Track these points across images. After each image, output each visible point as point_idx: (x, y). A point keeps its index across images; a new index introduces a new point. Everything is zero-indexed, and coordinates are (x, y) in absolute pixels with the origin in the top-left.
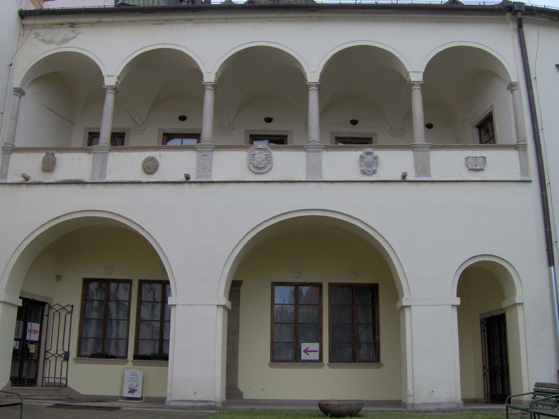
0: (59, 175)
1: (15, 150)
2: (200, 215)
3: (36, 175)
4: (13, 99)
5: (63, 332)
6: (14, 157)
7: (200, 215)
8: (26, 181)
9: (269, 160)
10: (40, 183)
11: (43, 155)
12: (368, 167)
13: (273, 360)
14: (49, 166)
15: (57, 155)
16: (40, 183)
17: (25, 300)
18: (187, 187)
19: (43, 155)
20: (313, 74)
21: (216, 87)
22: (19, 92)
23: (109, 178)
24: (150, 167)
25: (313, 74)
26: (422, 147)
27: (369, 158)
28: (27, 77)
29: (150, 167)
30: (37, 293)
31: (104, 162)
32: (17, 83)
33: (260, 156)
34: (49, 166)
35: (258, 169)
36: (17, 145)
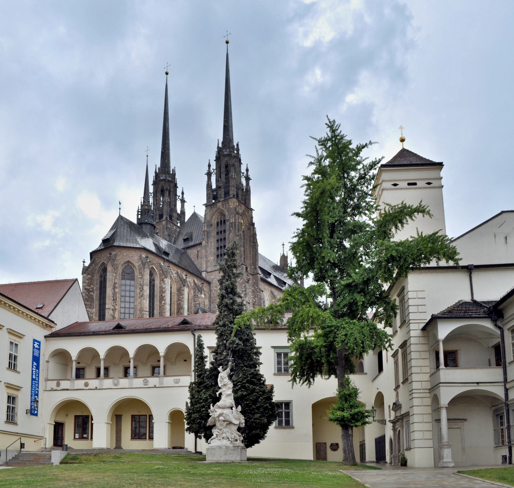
0: (62, 387)
1: (48, 380)
2: (100, 398)
3: (55, 388)
6: (48, 382)
7: (100, 398)
8: (52, 390)
9: (118, 382)
11: (56, 382)
12: (146, 383)
13: (132, 438)
14: (58, 385)
15: (60, 382)
17: (56, 423)
19: (56, 382)
20: (132, 354)
21: (104, 359)
22: (48, 362)
23: (76, 388)
24: (86, 385)
25: (132, 354)
26: (162, 376)
27: (145, 381)
28: (49, 357)
29: (86, 385)
31: (74, 384)
33: (116, 381)
34: (58, 385)
35: (115, 385)
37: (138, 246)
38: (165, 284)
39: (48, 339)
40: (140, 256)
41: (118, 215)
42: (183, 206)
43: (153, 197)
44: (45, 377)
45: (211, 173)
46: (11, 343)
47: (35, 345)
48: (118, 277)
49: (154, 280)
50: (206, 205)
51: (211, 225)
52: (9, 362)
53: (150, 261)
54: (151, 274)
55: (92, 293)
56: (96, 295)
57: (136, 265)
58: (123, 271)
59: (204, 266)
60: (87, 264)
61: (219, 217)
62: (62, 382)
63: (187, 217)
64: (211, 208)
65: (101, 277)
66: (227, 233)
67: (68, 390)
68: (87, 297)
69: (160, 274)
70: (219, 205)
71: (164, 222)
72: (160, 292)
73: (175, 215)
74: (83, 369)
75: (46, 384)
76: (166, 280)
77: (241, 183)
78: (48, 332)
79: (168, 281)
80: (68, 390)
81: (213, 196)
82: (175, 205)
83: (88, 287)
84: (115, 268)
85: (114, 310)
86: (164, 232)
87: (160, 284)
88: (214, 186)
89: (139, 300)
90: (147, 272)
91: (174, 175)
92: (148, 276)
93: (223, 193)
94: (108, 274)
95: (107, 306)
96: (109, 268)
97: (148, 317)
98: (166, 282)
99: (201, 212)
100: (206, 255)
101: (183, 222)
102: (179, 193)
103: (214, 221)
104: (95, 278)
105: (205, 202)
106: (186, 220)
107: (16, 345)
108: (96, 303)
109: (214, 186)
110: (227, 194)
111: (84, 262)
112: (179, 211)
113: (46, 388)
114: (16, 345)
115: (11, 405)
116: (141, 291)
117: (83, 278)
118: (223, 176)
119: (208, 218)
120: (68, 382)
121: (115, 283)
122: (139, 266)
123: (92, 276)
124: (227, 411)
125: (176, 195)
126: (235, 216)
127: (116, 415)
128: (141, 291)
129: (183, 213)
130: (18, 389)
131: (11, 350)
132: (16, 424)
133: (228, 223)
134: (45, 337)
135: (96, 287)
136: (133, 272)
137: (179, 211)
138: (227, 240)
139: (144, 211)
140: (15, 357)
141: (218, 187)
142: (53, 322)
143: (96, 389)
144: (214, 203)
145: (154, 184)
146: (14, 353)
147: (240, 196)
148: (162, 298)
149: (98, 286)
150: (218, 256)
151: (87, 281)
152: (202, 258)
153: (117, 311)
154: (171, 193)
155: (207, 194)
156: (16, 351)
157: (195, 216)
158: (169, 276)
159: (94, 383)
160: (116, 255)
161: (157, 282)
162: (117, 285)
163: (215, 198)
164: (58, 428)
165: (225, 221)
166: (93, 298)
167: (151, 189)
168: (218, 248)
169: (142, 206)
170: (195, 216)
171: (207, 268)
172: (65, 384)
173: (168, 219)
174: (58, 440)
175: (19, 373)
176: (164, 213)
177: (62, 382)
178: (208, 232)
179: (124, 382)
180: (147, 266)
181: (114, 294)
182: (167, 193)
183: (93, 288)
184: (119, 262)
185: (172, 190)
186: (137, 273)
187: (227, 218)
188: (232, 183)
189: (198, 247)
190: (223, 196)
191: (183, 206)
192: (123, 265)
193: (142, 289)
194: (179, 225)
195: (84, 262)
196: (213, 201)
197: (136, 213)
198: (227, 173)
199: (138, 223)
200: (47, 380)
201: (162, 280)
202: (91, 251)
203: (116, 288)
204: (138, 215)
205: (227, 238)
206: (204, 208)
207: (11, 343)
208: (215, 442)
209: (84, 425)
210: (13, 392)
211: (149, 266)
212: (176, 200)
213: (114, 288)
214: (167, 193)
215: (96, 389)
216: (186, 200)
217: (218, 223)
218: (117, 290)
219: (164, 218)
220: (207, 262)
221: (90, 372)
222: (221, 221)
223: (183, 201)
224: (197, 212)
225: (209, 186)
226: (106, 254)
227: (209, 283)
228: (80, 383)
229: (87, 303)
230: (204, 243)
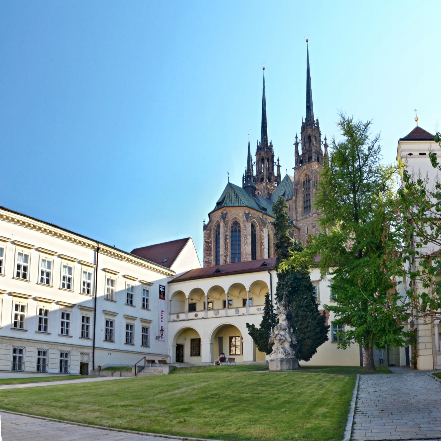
1: (171, 314)
3: (176, 319)
4: (170, 303)
5: (187, 351)
8: (174, 321)
10: (176, 321)
11: (176, 315)
16: (176, 321)
18: (203, 320)
19: (176, 315)
22: (171, 301)
23: (189, 318)
24: (196, 315)
28: (172, 297)
29: (196, 315)
30: (180, 342)
32: (170, 299)
34: (178, 317)
35: (216, 315)
36: (172, 312)
37: (242, 205)
38: (263, 233)
39: (170, 284)
40: (245, 213)
41: (227, 183)
42: (279, 170)
43: (256, 165)
44: (169, 311)
45: (298, 143)
46: (144, 290)
47: (161, 289)
48: (228, 231)
49: (255, 231)
50: (295, 168)
51: (299, 184)
52: (143, 304)
53: (252, 216)
54: (253, 226)
55: (210, 245)
56: (213, 246)
57: (242, 220)
58: (232, 227)
59: (295, 216)
60: (206, 223)
61: (305, 178)
62: (180, 315)
63: (282, 178)
64: (298, 170)
65: (217, 231)
66: (311, 189)
67: (184, 320)
68: (207, 248)
69: (260, 225)
70: (305, 167)
71: (264, 184)
72: (260, 239)
73: (273, 178)
74: (195, 304)
75: (170, 317)
76: (264, 229)
77: (320, 149)
78: (170, 280)
79: (265, 230)
80: (184, 320)
81: (301, 161)
82: (273, 169)
83: (207, 240)
84: (226, 224)
85: (226, 256)
86: (264, 192)
87: (260, 233)
88: (300, 153)
89: (244, 247)
90: (250, 225)
91: (271, 146)
92: (250, 228)
93: (307, 158)
94: (221, 229)
95: (221, 253)
96: (222, 224)
97: (251, 259)
98: (264, 231)
99: (292, 174)
100: (296, 208)
101: (278, 183)
102: (275, 160)
103: (302, 180)
104: (212, 232)
105: (294, 166)
106: (281, 180)
107: (148, 291)
108: (213, 252)
109: (300, 153)
110: (310, 159)
111: (204, 221)
112: (276, 175)
113: (170, 319)
114: (148, 291)
115: (145, 334)
116: (245, 240)
117: (205, 233)
118: (307, 145)
119: (297, 178)
120: (184, 314)
121: (226, 235)
122: (244, 220)
123: (211, 232)
124: (282, 333)
125: (273, 162)
126: (316, 176)
127: (219, 338)
128: (245, 240)
129: (279, 175)
130: (149, 322)
131: (144, 295)
132: (149, 347)
133: (311, 182)
134: (169, 283)
135: (213, 239)
136: (239, 227)
137: (276, 175)
138: (311, 196)
139: (247, 177)
140: (147, 300)
141: (303, 154)
142: (174, 272)
143: (203, 318)
144: (301, 166)
145: (257, 154)
146: (146, 297)
147: (320, 160)
148: (262, 244)
149: (215, 239)
150: (305, 208)
151: (207, 236)
152: (293, 210)
153: (228, 256)
154: (270, 161)
155: (295, 160)
156: (148, 296)
157: (287, 177)
158: (266, 226)
159: (201, 314)
160: (226, 214)
161: (258, 232)
162: (228, 237)
163: (301, 162)
164: (179, 348)
165: (309, 180)
166: (211, 248)
167: (254, 159)
168: (304, 202)
169: (246, 173)
170: (287, 177)
171: (297, 217)
172: (182, 316)
173: (267, 181)
174: (179, 357)
175: (150, 310)
176: (265, 177)
177: (180, 315)
178: (297, 190)
179: (222, 312)
180: (249, 220)
181: (226, 244)
182: (266, 161)
183: (211, 241)
184: (229, 218)
185: (270, 158)
186: (242, 226)
187: (310, 178)
188: (314, 150)
189: (290, 201)
190: (307, 160)
191: (279, 170)
192: (232, 221)
193: (246, 238)
194: (276, 185)
195: (204, 221)
196: (300, 165)
197: (242, 179)
198: (310, 142)
199: (244, 188)
200: (171, 314)
201: (261, 230)
202: (209, 213)
203: (227, 239)
204: (243, 181)
205: (311, 193)
206: (293, 170)
207: (144, 290)
208: (273, 356)
209: (196, 345)
210: (146, 325)
211: (251, 220)
212: (273, 166)
213: (226, 239)
214: (266, 161)
215: (203, 318)
216: (281, 165)
217: (304, 182)
218: (228, 241)
219: (265, 180)
220: (296, 213)
221: (199, 306)
222: (306, 180)
223: (279, 166)
224: (289, 174)
225: (297, 152)
226: (219, 213)
227: (299, 229)
228: (192, 315)
229: (208, 252)
230: (294, 198)
